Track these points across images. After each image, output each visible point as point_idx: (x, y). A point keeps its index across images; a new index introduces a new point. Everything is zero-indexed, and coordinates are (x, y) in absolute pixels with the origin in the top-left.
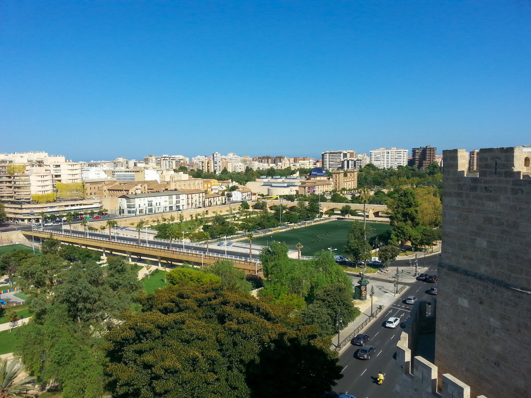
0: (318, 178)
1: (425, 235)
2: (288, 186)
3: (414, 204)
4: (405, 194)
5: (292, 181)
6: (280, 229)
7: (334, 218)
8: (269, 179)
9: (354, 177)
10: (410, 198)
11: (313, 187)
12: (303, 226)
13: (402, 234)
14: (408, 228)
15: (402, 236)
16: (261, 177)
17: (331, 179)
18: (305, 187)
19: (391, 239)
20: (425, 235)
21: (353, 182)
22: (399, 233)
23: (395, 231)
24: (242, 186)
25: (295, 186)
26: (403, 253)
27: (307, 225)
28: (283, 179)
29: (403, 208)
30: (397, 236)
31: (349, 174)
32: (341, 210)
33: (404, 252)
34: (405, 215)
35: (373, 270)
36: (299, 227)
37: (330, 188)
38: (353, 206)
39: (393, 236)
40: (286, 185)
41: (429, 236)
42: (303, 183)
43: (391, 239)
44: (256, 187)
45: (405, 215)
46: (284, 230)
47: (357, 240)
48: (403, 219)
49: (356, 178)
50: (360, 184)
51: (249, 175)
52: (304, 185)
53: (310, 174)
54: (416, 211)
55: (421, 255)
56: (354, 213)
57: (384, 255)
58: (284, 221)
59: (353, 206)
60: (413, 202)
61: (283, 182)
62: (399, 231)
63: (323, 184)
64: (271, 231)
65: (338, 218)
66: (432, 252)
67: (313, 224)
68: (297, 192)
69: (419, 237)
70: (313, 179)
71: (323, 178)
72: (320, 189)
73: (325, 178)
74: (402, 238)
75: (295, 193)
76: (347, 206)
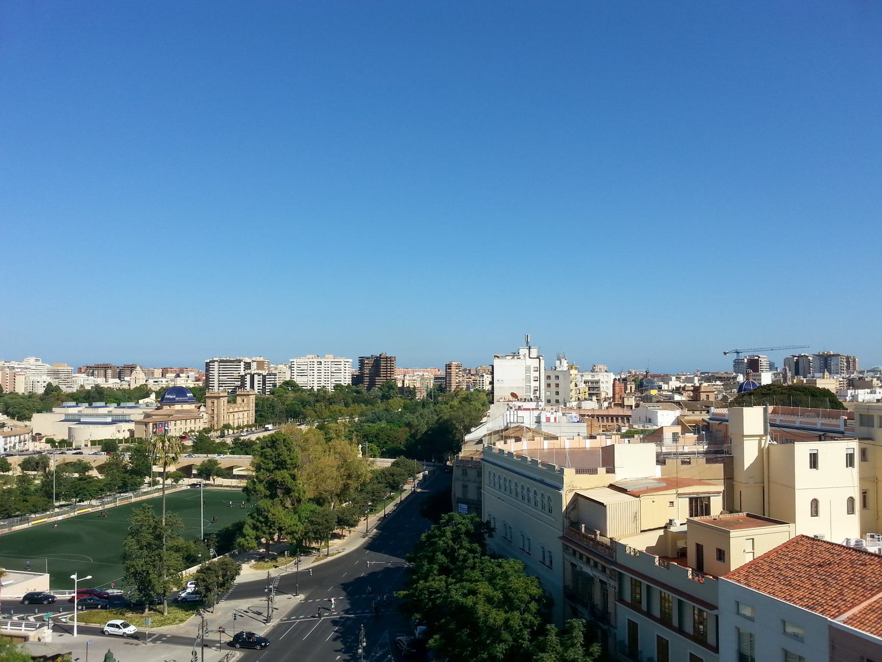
0: (178, 407)
1: (312, 522)
2: (114, 422)
3: (289, 461)
4: (274, 442)
5: (126, 411)
6: (58, 514)
7: (185, 483)
8: (83, 408)
9: (248, 403)
10: (283, 449)
11: (166, 422)
12: (107, 506)
13: (264, 522)
14: (280, 513)
15: (264, 528)
16: (65, 404)
17: (202, 409)
18: (146, 424)
19: (244, 536)
20: (312, 522)
21: (246, 413)
22: (261, 522)
23: (253, 518)
24: (15, 422)
25: (122, 421)
26: (270, 564)
27: (118, 503)
28: (112, 408)
29: (268, 470)
30: (255, 528)
31: (239, 399)
32: (198, 470)
33: (274, 558)
34: (272, 485)
35: (180, 614)
36: (100, 508)
37: (201, 425)
38: (224, 460)
39: (248, 530)
40: (109, 420)
41: (319, 524)
42: (147, 416)
43: (244, 536)
44: (49, 424)
45: (272, 485)
46: (60, 518)
47: (145, 552)
48: (268, 493)
49: (252, 406)
50: (261, 416)
51: (51, 398)
52: (147, 420)
53: (162, 400)
54: (294, 477)
55: (308, 563)
56: (227, 473)
57: (204, 580)
58: (67, 497)
59: (224, 460)
60: (287, 458)
61: (110, 414)
62: (261, 518)
63: (187, 416)
64: (27, 520)
65: (193, 485)
66: (327, 555)
67: (133, 500)
68: (132, 432)
69: (301, 527)
70: (166, 408)
71: (186, 407)
72: (178, 427)
73: (192, 407)
74: (264, 533)
75: (127, 435)
76: (209, 461)
